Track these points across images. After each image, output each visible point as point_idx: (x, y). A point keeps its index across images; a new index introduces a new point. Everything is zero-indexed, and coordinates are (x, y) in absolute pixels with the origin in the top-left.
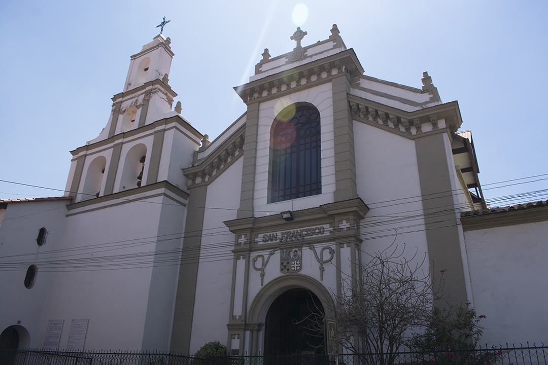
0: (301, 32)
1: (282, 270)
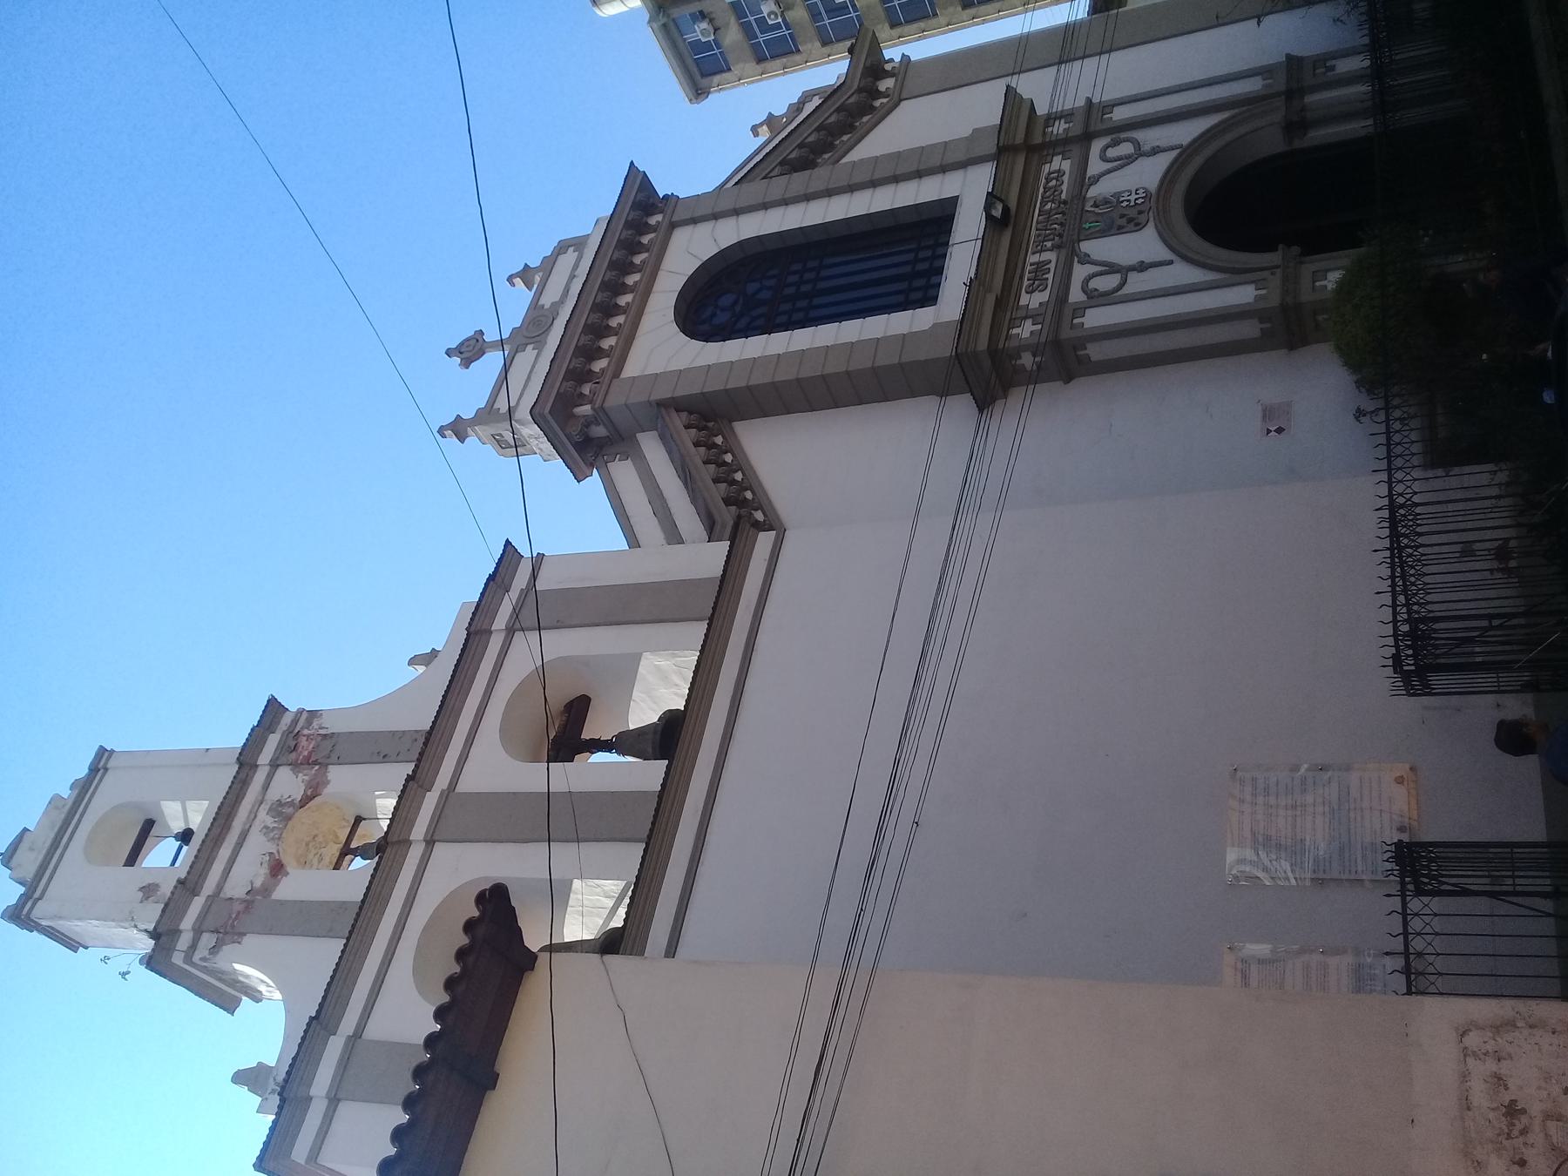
0: (468, 340)
1: (1137, 224)
